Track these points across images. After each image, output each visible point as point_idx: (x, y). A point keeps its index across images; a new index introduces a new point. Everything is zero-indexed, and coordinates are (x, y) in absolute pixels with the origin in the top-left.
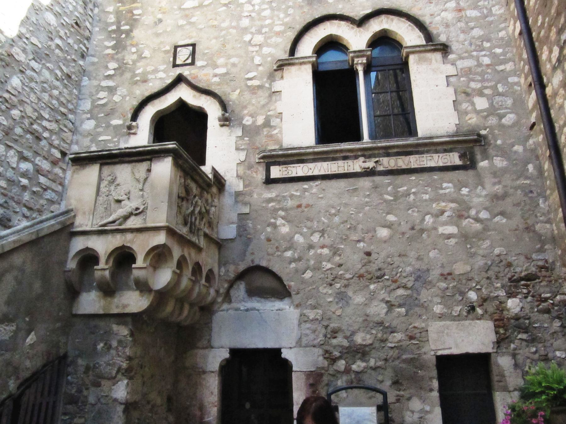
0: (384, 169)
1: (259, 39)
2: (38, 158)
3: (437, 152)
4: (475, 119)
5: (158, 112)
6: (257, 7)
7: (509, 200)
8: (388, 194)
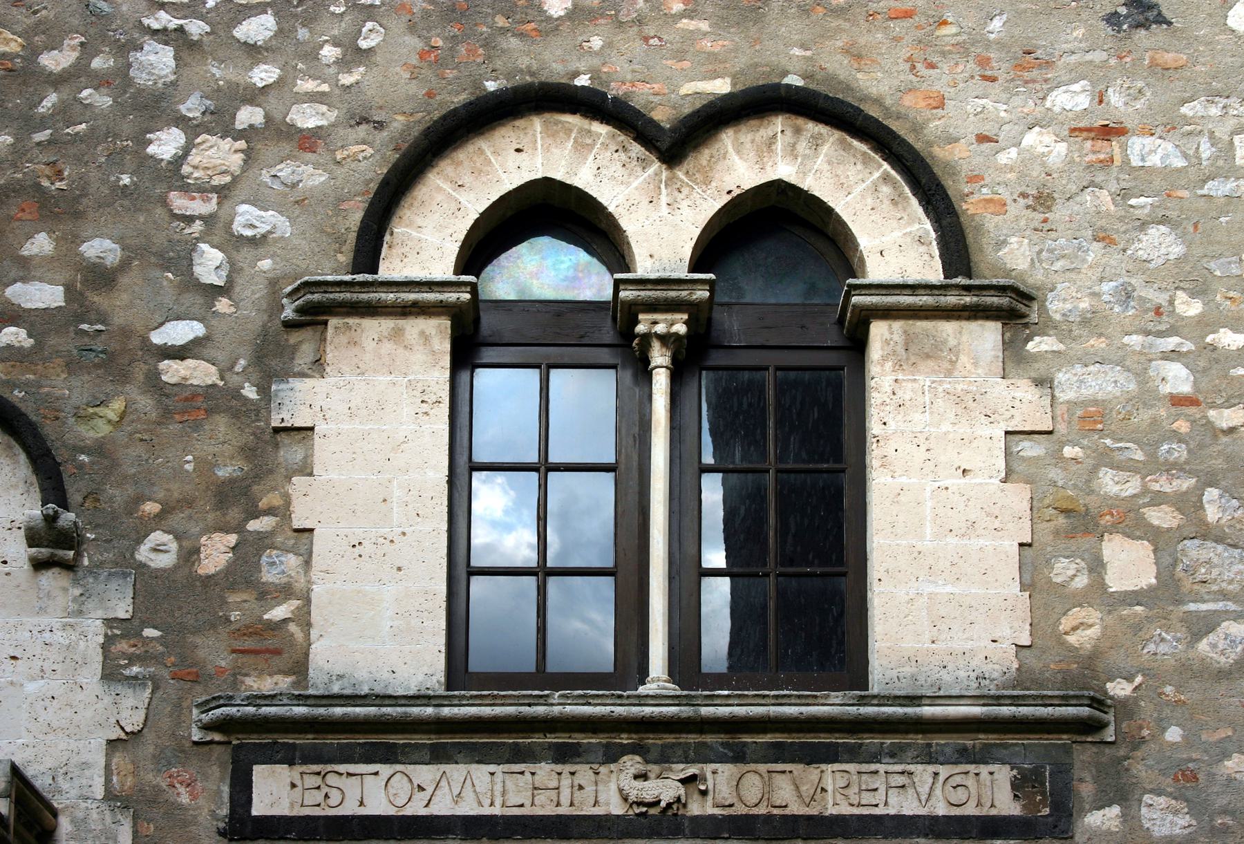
0: (717, 811)
1: (218, 155)
3: (929, 757)
4: (1094, 632)
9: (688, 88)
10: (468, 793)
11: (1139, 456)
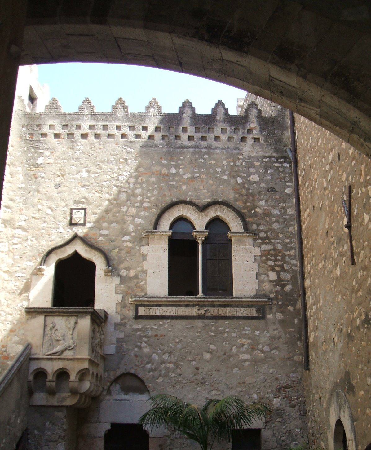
0: (210, 315)
1: (133, 211)
4: (268, 287)
7: (281, 340)
8: (211, 331)
9: (204, 200)
10: (172, 312)
11: (274, 259)
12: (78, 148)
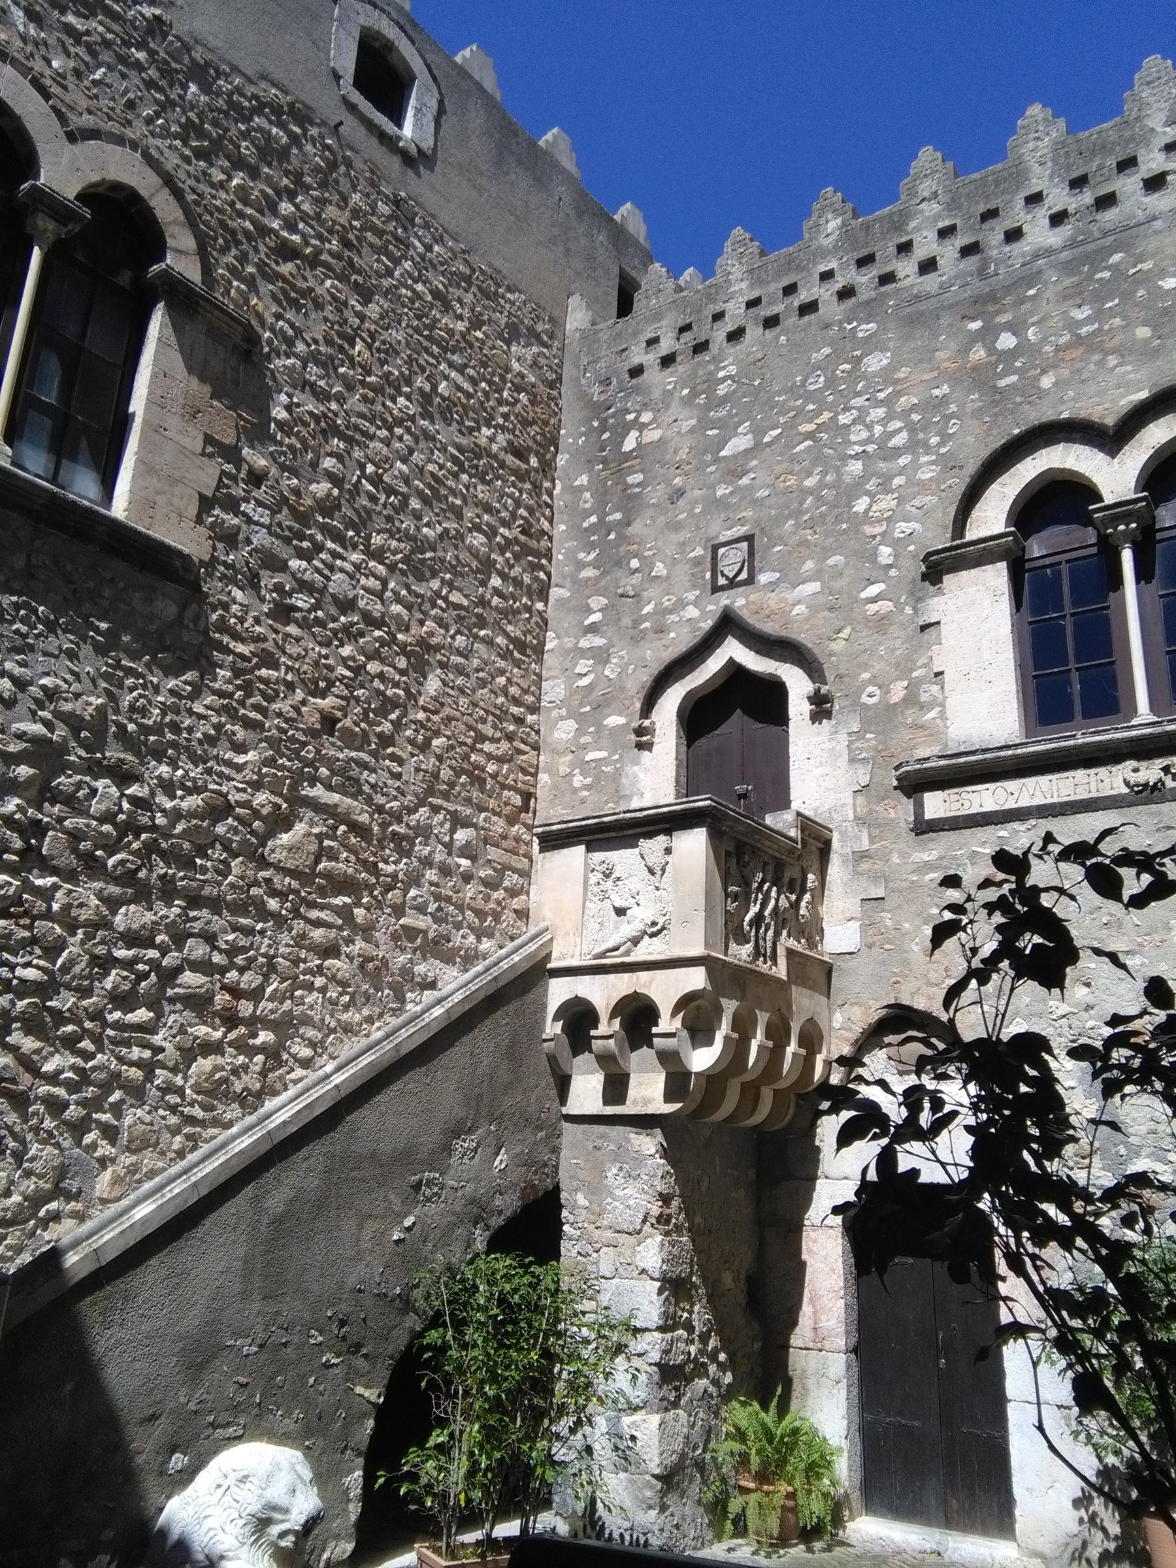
1: (887, 502)
2: (483, 815)
5: (689, 695)
6: (878, 429)
10: (1038, 793)
12: (721, 374)
